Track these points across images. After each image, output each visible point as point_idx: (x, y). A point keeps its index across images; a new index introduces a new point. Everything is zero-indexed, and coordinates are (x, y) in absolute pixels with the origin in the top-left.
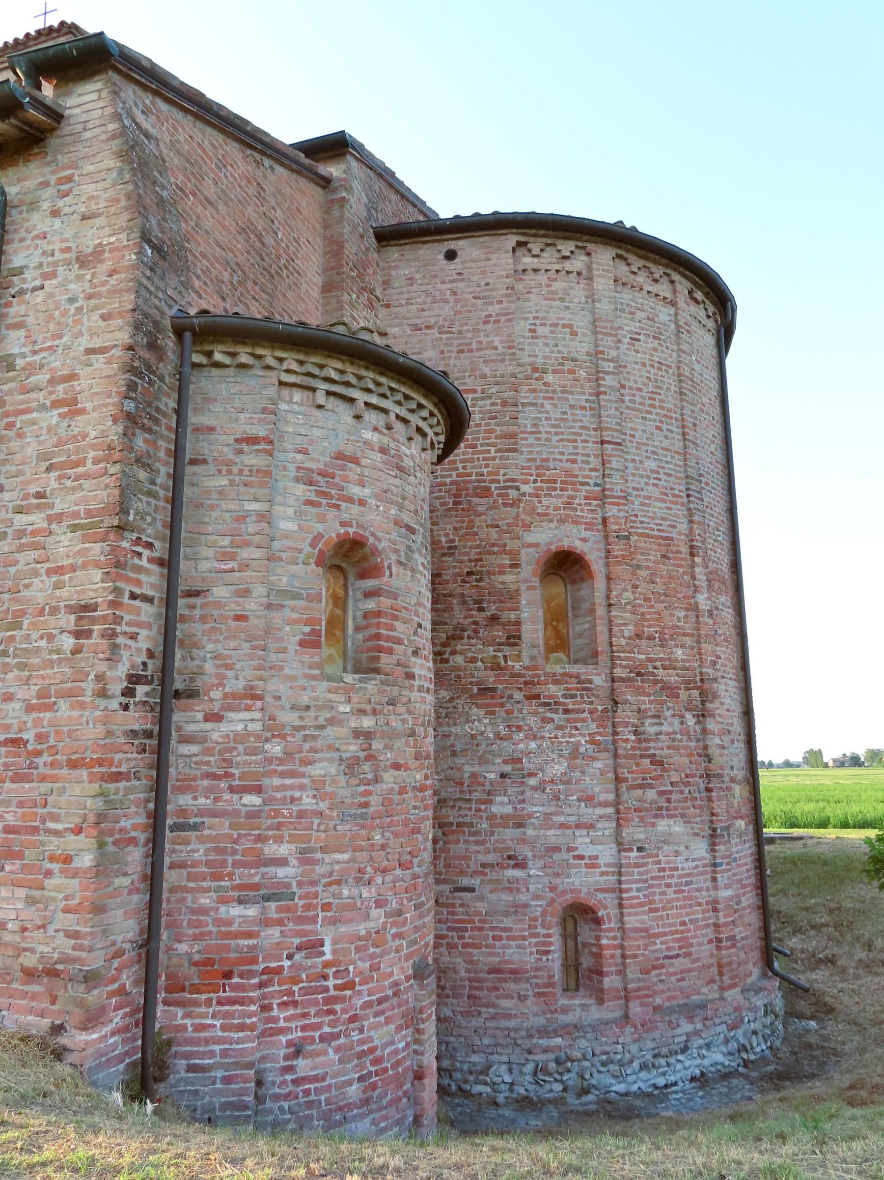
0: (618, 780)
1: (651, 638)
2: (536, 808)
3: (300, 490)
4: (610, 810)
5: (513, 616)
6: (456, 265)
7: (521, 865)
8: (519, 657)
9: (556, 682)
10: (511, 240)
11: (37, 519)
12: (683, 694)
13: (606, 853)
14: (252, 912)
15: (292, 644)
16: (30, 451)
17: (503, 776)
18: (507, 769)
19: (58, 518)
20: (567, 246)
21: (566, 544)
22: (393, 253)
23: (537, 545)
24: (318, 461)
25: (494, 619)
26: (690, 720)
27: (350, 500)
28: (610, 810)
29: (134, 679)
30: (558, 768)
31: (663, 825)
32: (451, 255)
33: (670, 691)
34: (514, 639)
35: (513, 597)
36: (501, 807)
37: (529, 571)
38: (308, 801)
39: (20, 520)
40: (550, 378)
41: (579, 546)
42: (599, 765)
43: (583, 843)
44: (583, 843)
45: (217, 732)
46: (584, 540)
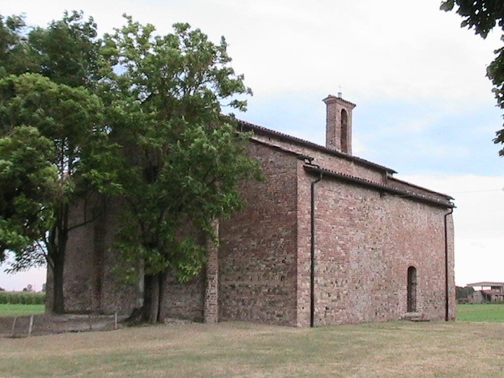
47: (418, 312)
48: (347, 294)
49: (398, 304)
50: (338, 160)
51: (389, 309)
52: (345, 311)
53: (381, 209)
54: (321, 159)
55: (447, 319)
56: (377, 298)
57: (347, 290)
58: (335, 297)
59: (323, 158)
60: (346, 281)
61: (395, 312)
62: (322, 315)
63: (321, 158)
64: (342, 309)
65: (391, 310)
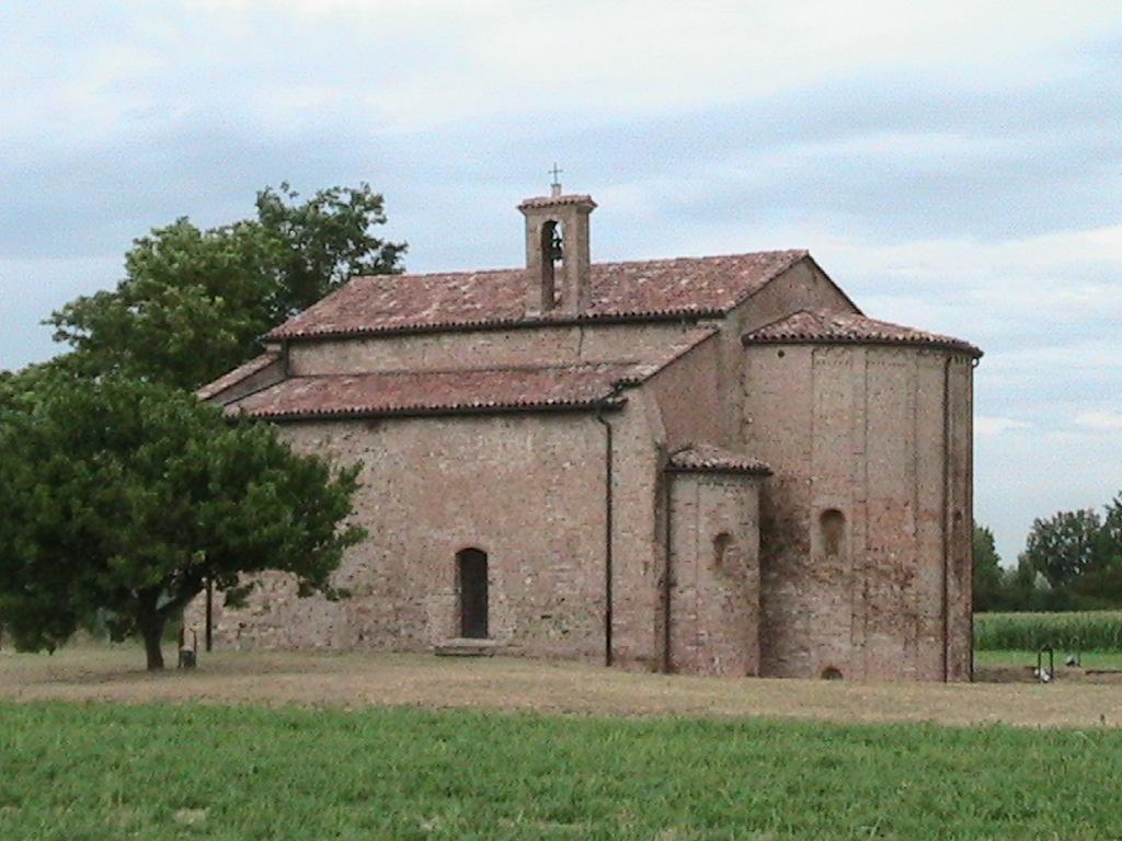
0: (854, 615)
1: (876, 549)
2: (814, 626)
3: (706, 519)
4: (848, 629)
5: (806, 541)
6: (782, 361)
7: (807, 650)
8: (809, 560)
9: (826, 571)
10: (810, 349)
11: (629, 535)
12: (893, 576)
13: (846, 647)
14: (694, 648)
15: (704, 568)
16: (626, 514)
17: (800, 612)
18: (802, 609)
19: (637, 535)
20: (839, 350)
21: (832, 506)
22: (753, 352)
23: (818, 507)
24: (713, 506)
25: (798, 542)
26: (897, 588)
27: (722, 519)
28: (848, 629)
29: (661, 582)
30: (825, 609)
31: (876, 636)
32: (781, 354)
33: (884, 574)
34: (806, 551)
35: (807, 531)
36: (799, 625)
37: (815, 518)
38: (710, 617)
39: (624, 534)
40: (828, 421)
41: (839, 507)
42: (844, 609)
43: (835, 641)
44: (835, 641)
45: (682, 596)
46: (842, 504)
47: (492, 639)
48: (286, 604)
49: (424, 622)
50: (533, 334)
51: (398, 631)
52: (280, 631)
53: (373, 451)
54: (483, 345)
55: (609, 662)
56: (361, 611)
57: (286, 598)
58: (259, 609)
59: (488, 342)
60: (285, 583)
61: (416, 636)
62: (232, 636)
63: (482, 342)
64: (275, 627)
65: (403, 632)
